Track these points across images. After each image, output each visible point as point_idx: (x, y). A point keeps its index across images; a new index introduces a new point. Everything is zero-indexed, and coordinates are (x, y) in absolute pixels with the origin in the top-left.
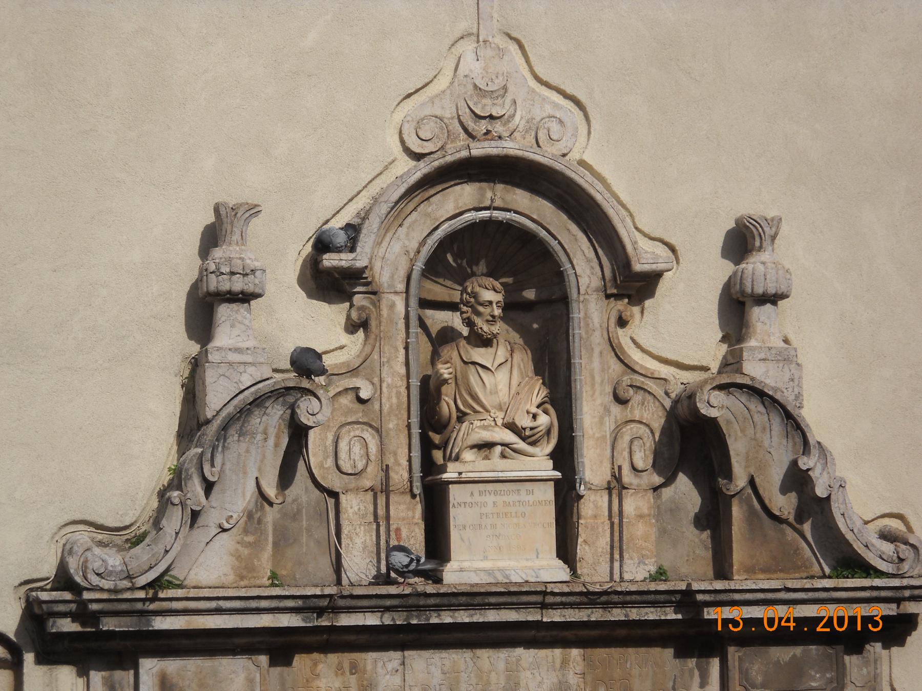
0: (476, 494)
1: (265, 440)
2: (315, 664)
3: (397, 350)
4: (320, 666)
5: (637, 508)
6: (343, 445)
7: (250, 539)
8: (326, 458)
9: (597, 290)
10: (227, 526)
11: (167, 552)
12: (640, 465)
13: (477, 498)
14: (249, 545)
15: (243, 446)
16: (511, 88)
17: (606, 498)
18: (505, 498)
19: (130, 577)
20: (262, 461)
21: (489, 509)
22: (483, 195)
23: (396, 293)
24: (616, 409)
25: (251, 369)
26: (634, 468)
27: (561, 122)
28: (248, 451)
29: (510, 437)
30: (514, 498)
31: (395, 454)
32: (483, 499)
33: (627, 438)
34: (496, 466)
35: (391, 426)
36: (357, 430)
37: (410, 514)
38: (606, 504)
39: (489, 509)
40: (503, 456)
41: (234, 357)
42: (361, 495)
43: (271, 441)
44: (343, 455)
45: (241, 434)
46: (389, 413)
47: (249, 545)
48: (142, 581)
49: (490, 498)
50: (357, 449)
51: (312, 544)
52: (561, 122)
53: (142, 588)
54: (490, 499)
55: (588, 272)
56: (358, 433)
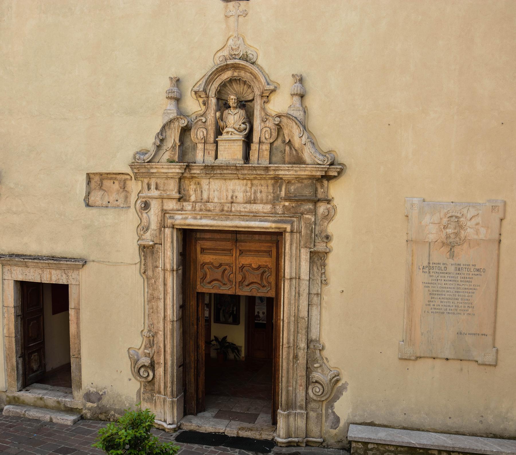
0: (224, 143)
1: (175, 130)
2: (190, 182)
3: (212, 111)
4: (191, 183)
5: (266, 148)
6: (198, 132)
7: (173, 153)
8: (195, 136)
9: (260, 95)
10: (167, 150)
11: (151, 155)
12: (267, 137)
13: (224, 144)
14: (173, 154)
15: (170, 131)
16: (240, 47)
17: (258, 145)
18: (231, 144)
19: (144, 160)
20: (175, 135)
21: (227, 147)
22: (233, 74)
23: (212, 97)
24: (262, 124)
25: (172, 114)
26: (266, 138)
27: (253, 55)
28: (171, 132)
29: (233, 130)
30: (233, 144)
31: (210, 135)
32: (226, 144)
33: (264, 131)
34: (229, 137)
35: (209, 128)
36: (202, 129)
37: (212, 148)
38: (258, 147)
39: (227, 147)
40: (231, 135)
41: (169, 111)
42: (202, 144)
43: (176, 130)
44: (198, 135)
45: (169, 129)
46: (209, 125)
47: (173, 154)
48: (146, 161)
49: (227, 144)
50: (201, 133)
51: (192, 155)
52: (253, 55)
53: (146, 162)
54: (227, 144)
55: (258, 91)
56: (202, 130)
